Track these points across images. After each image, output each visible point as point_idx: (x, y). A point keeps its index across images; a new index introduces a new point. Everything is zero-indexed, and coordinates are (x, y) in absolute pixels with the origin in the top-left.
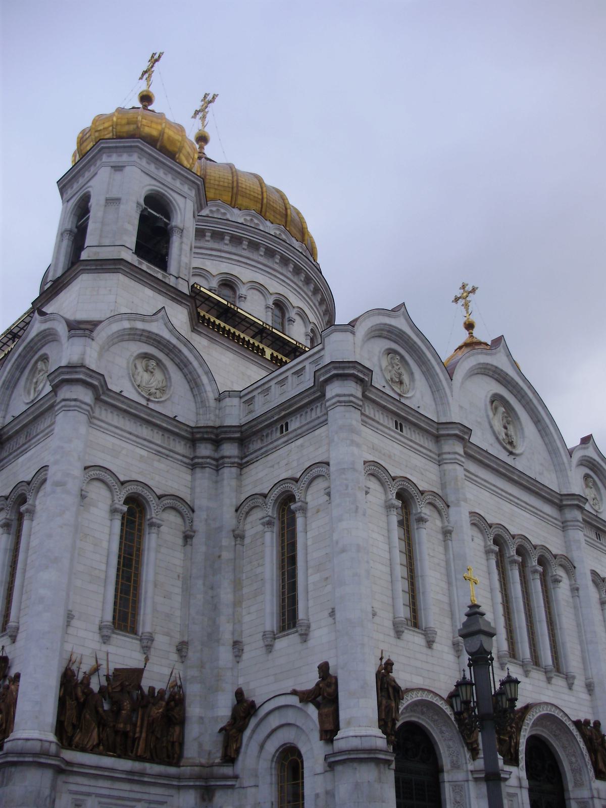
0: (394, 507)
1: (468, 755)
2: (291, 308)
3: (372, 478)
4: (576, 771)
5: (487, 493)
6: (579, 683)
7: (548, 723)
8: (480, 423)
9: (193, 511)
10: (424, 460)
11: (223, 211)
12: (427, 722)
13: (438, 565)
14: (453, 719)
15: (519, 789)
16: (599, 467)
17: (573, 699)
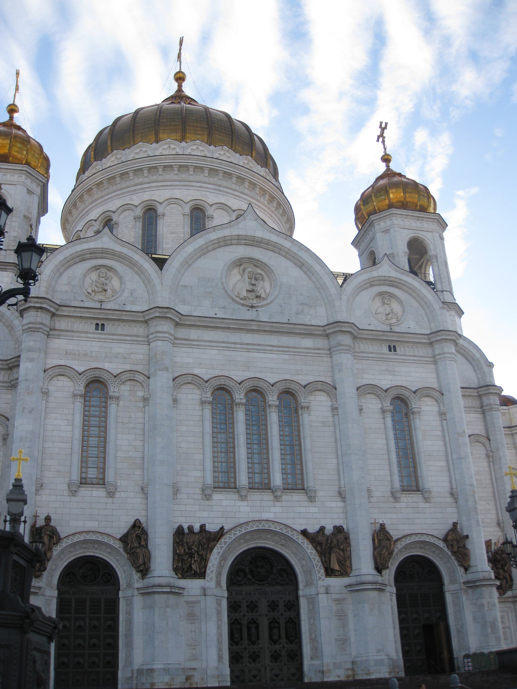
0: (77, 396)
1: (136, 576)
2: (209, 207)
3: (60, 378)
4: (308, 572)
5: (215, 352)
6: (326, 494)
7: (269, 536)
8: (210, 293)
9: (8, 420)
10: (129, 346)
11: (144, 149)
12: (103, 555)
13: (134, 428)
14: (122, 550)
15: (203, 597)
16: (399, 281)
17: (315, 510)
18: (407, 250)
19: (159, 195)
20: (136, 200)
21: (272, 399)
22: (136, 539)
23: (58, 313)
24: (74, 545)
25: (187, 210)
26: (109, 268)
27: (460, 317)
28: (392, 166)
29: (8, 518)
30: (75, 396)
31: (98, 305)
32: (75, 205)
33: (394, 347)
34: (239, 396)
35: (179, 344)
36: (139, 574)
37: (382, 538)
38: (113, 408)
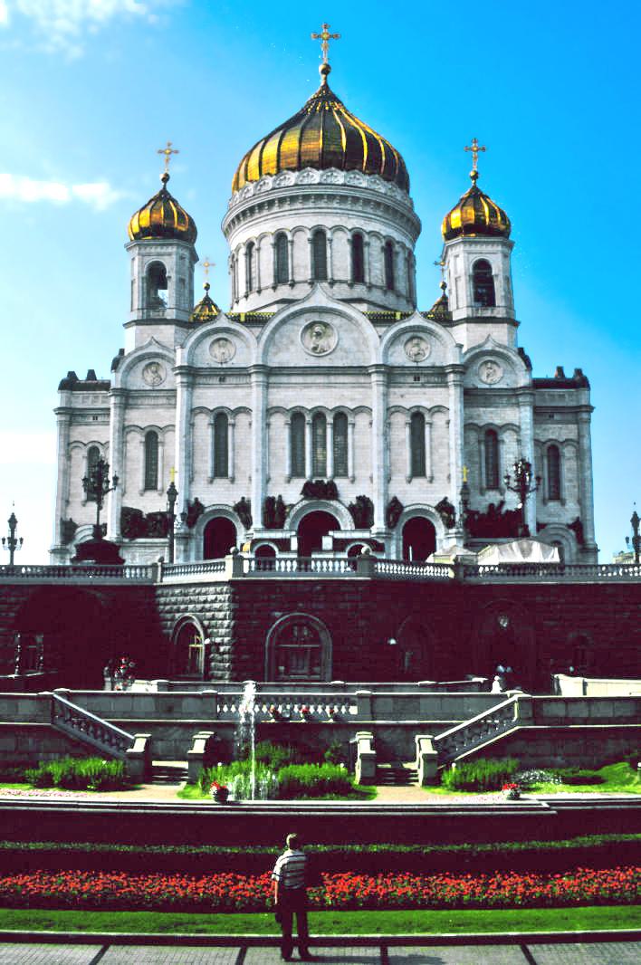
21: (330, 419)
22: (243, 508)
24: (210, 512)
26: (226, 340)
31: (220, 366)
37: (394, 508)
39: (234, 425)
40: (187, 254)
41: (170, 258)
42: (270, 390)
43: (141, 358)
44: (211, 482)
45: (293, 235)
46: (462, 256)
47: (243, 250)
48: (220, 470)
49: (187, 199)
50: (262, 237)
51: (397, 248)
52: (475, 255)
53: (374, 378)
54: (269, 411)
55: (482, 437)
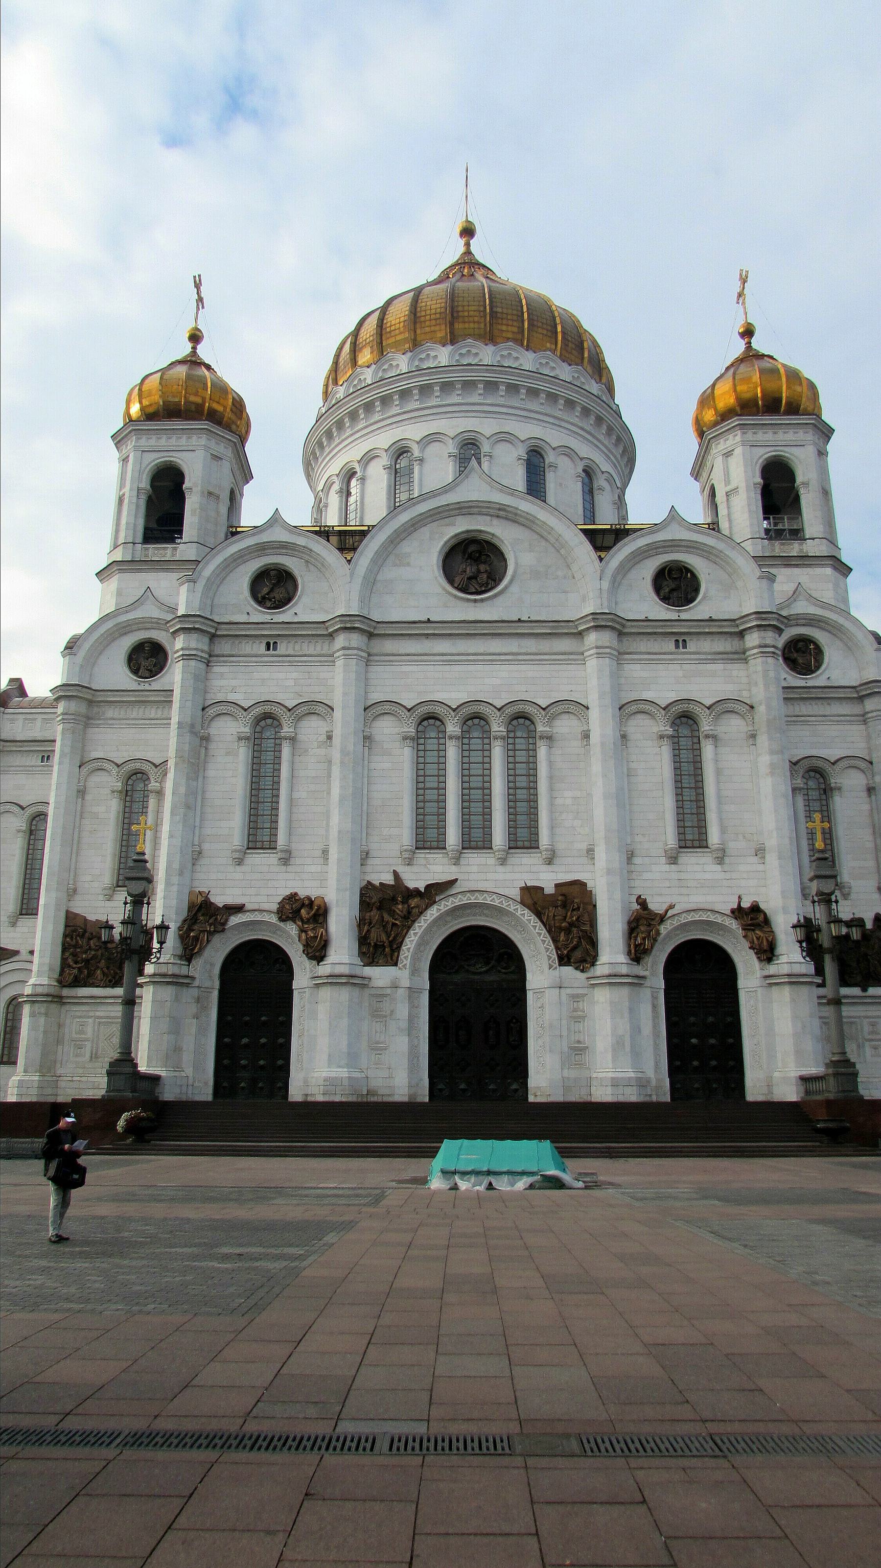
18: (759, 480)
19: (413, 432)
20: (384, 439)
21: (497, 727)
23: (219, 633)
25: (451, 447)
27: (846, 576)
28: (757, 344)
29: (129, 899)
30: (240, 739)
32: (313, 453)
33: (684, 641)
34: (453, 727)
35: (377, 661)
36: (315, 962)
38: (286, 751)
39: (293, 740)
40: (227, 452)
41: (194, 455)
42: (371, 668)
43: (124, 629)
44: (240, 862)
45: (422, 450)
46: (738, 451)
47: (336, 487)
48: (260, 833)
49: (233, 367)
50: (368, 459)
51: (600, 481)
52: (761, 451)
53: (592, 638)
54: (372, 711)
55: (799, 782)
